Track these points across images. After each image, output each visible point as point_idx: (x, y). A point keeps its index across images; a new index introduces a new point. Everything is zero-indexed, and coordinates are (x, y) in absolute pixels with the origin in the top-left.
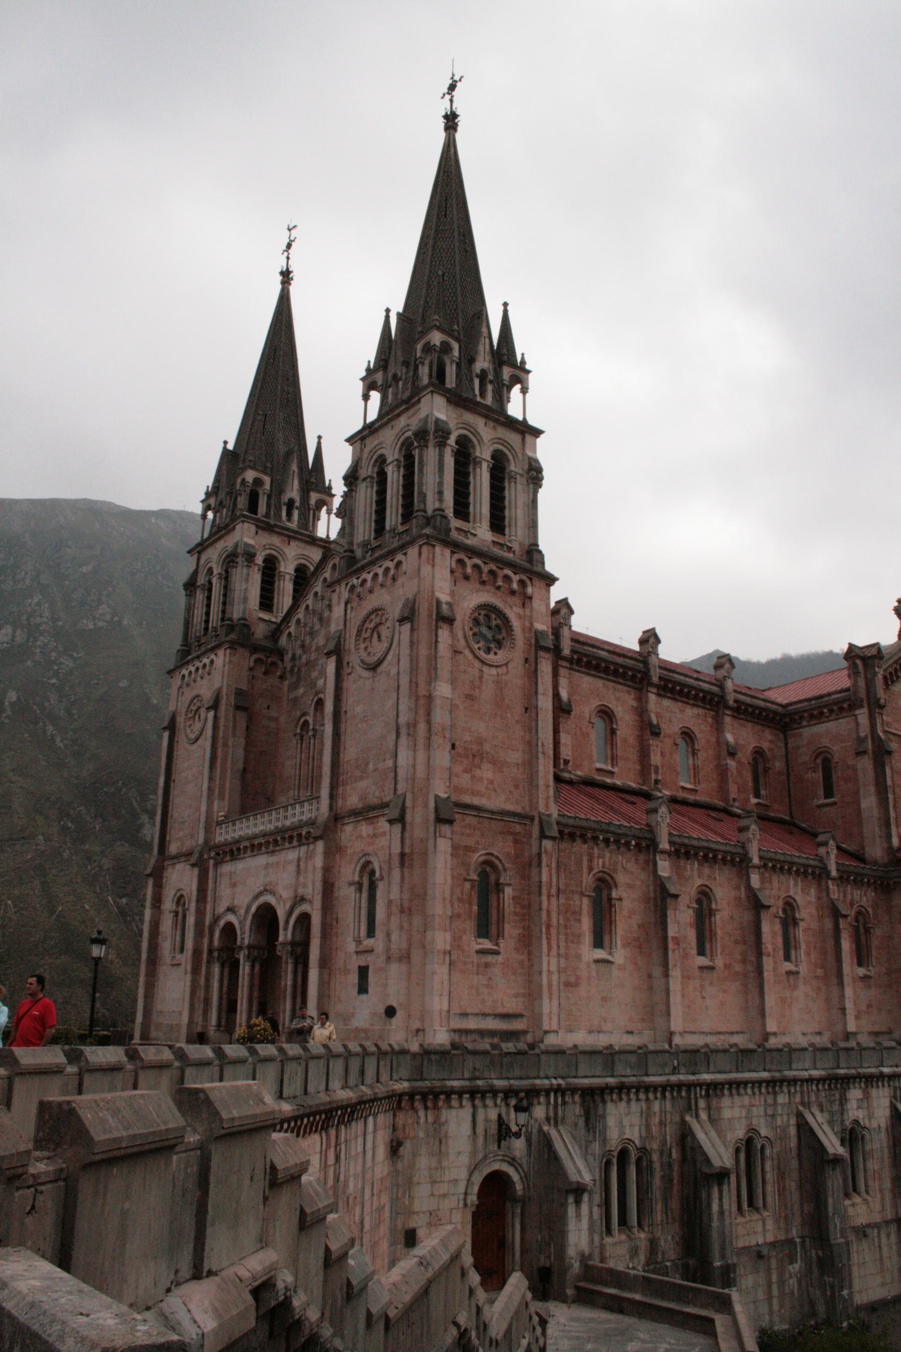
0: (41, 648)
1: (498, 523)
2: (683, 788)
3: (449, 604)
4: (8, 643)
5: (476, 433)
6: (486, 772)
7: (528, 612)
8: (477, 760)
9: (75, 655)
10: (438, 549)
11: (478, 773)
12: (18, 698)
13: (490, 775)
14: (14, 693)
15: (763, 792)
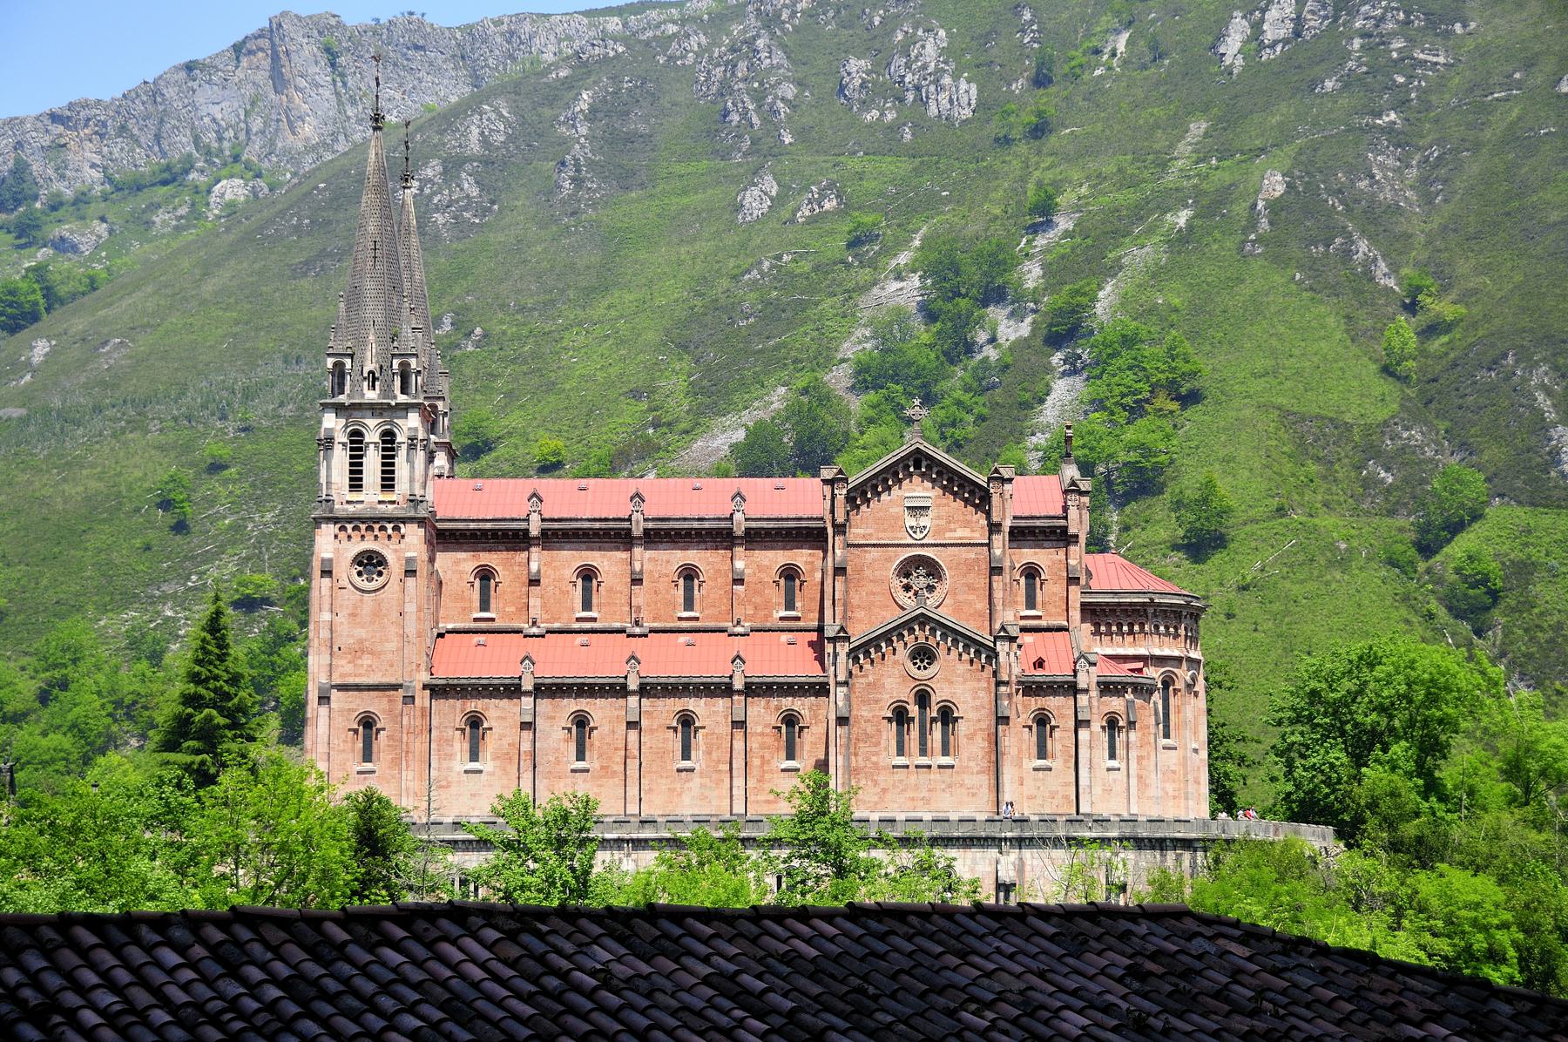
0: (1362, 36)
1: (388, 483)
2: (680, 619)
3: (330, 560)
4: (1286, 41)
5: (364, 425)
6: (366, 660)
7: (402, 546)
8: (359, 654)
9: (1458, 28)
10: (323, 526)
11: (360, 662)
12: (1290, 186)
13: (369, 662)
14: (1279, 178)
15: (798, 604)
